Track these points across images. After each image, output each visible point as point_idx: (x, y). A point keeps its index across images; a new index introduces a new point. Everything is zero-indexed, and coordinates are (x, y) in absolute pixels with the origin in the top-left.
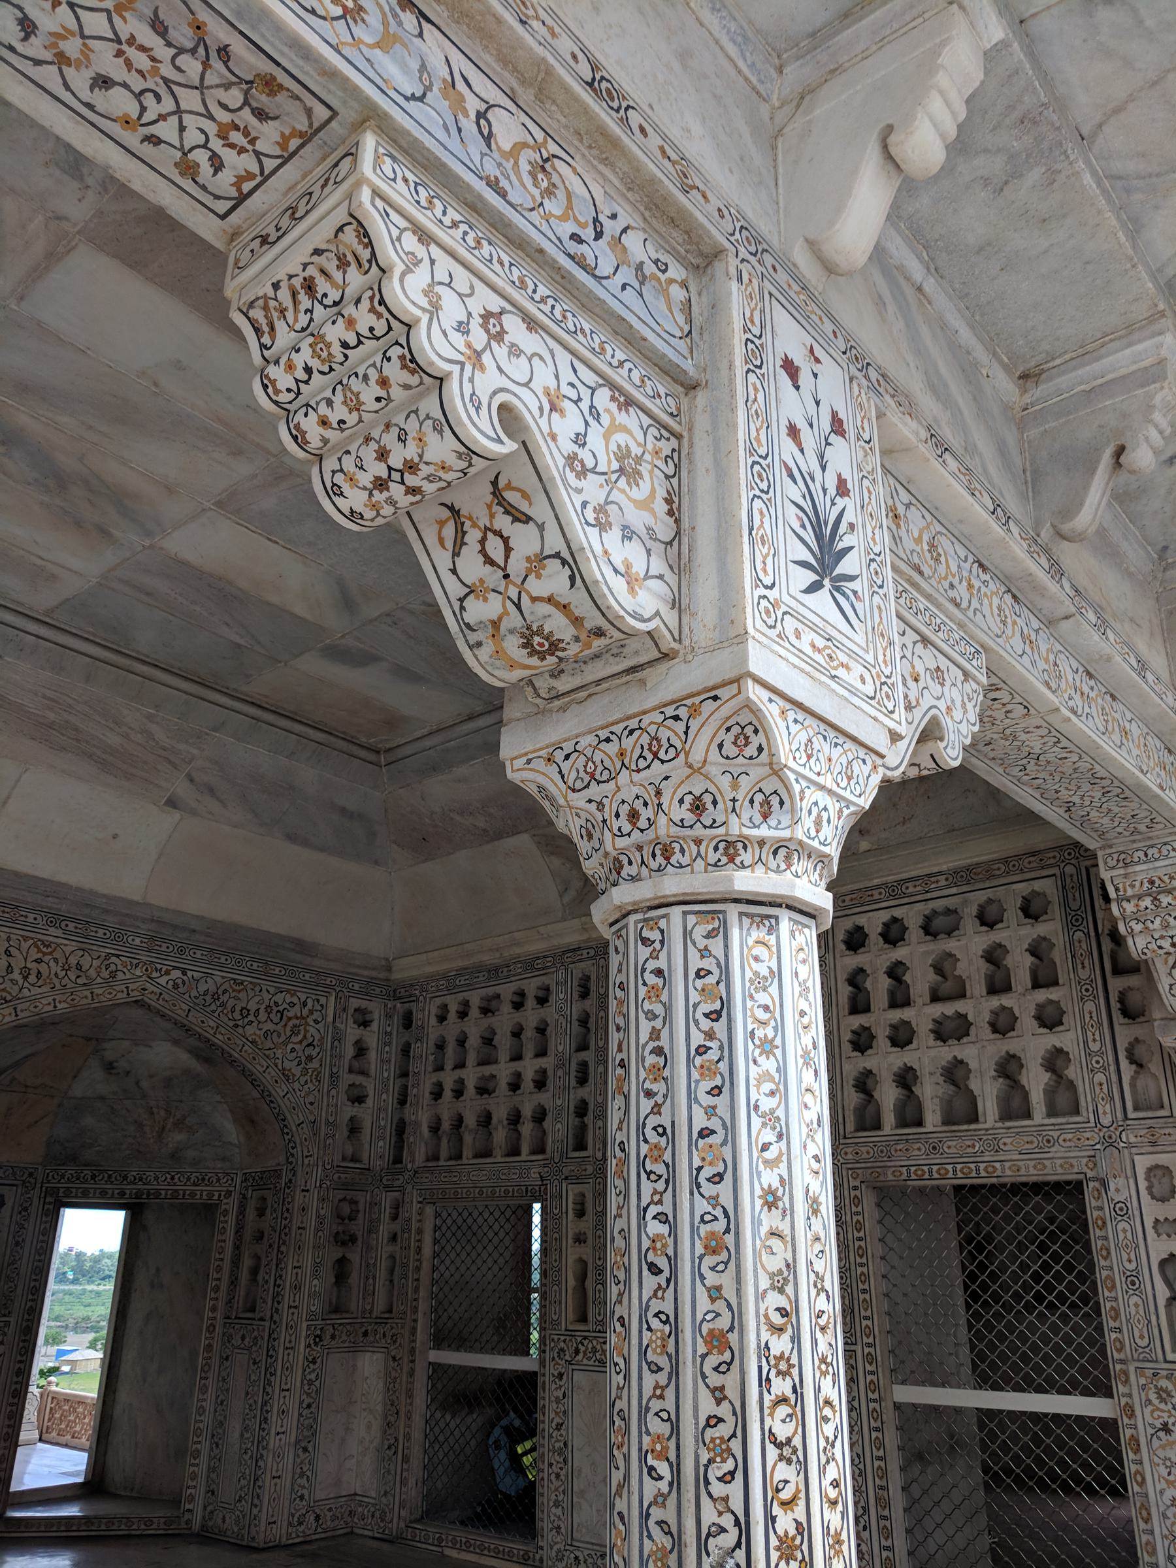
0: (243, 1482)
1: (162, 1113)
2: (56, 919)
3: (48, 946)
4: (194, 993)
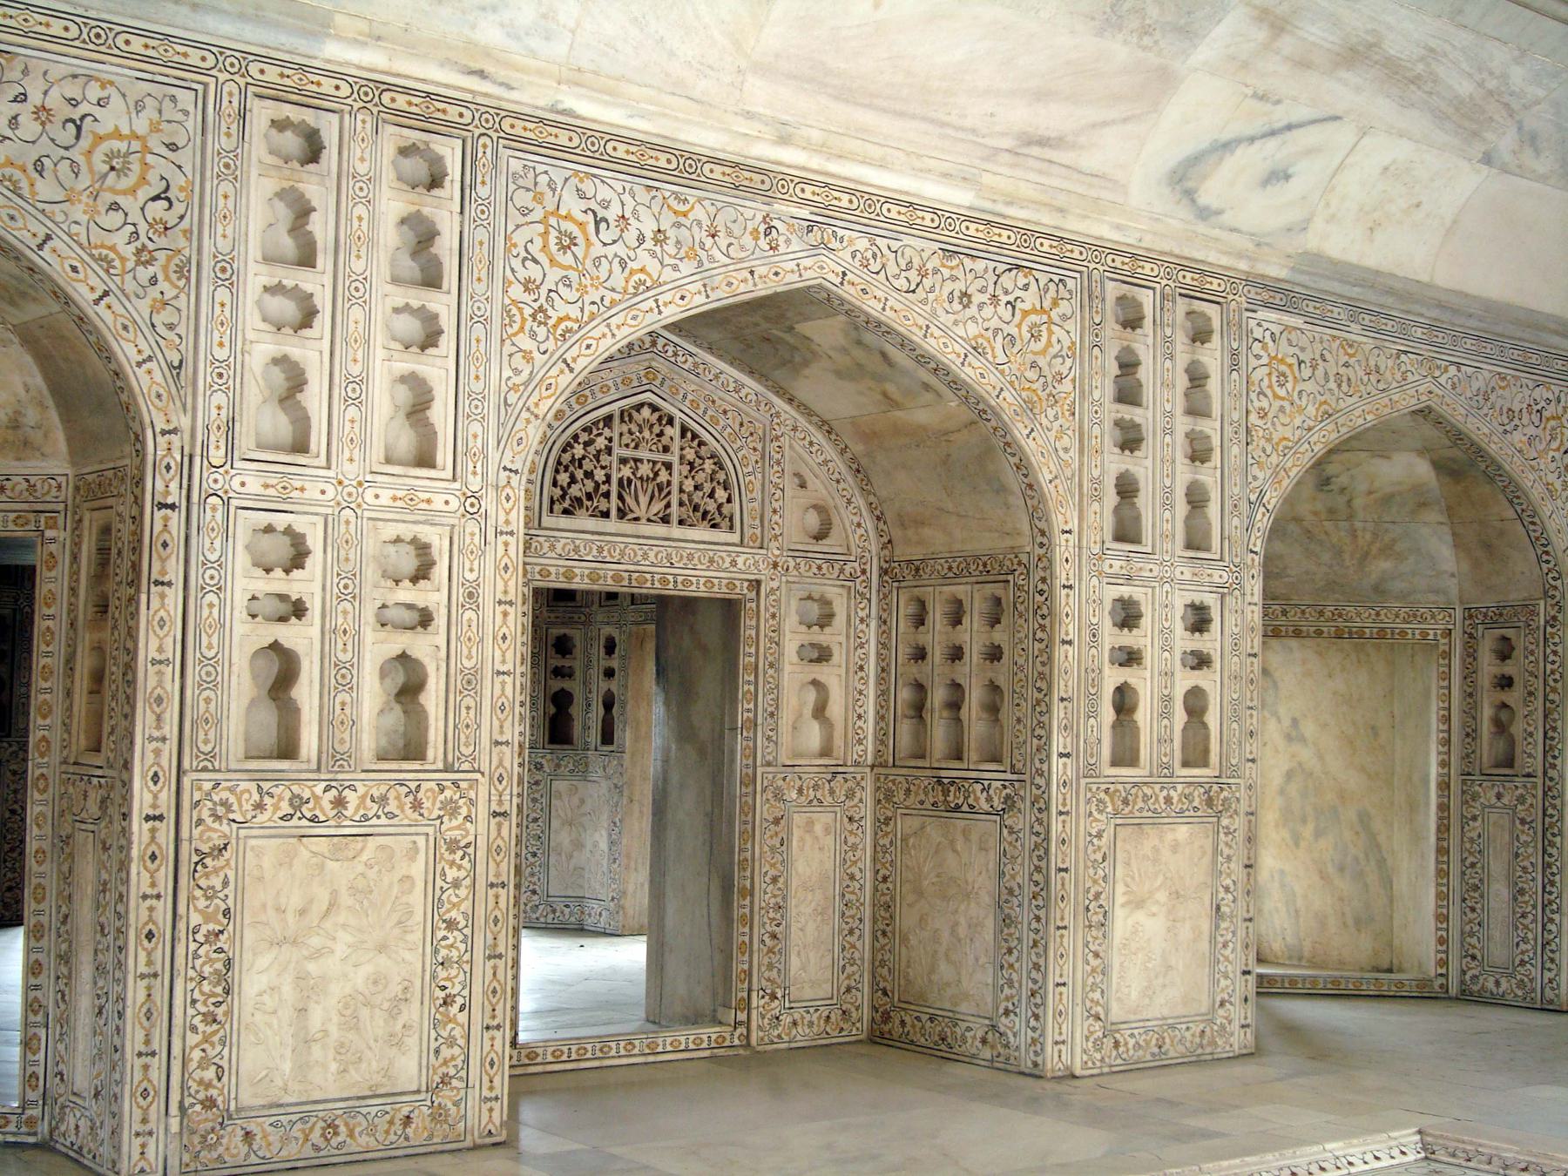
0: (1523, 946)
1: (1368, 536)
2: (1356, 309)
3: (1351, 346)
4: (1469, 395)
